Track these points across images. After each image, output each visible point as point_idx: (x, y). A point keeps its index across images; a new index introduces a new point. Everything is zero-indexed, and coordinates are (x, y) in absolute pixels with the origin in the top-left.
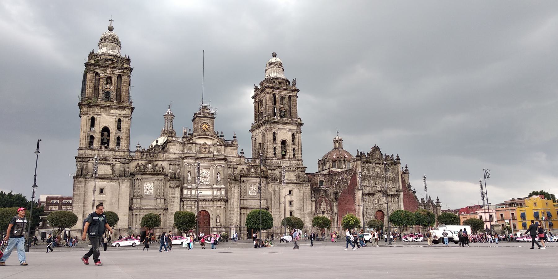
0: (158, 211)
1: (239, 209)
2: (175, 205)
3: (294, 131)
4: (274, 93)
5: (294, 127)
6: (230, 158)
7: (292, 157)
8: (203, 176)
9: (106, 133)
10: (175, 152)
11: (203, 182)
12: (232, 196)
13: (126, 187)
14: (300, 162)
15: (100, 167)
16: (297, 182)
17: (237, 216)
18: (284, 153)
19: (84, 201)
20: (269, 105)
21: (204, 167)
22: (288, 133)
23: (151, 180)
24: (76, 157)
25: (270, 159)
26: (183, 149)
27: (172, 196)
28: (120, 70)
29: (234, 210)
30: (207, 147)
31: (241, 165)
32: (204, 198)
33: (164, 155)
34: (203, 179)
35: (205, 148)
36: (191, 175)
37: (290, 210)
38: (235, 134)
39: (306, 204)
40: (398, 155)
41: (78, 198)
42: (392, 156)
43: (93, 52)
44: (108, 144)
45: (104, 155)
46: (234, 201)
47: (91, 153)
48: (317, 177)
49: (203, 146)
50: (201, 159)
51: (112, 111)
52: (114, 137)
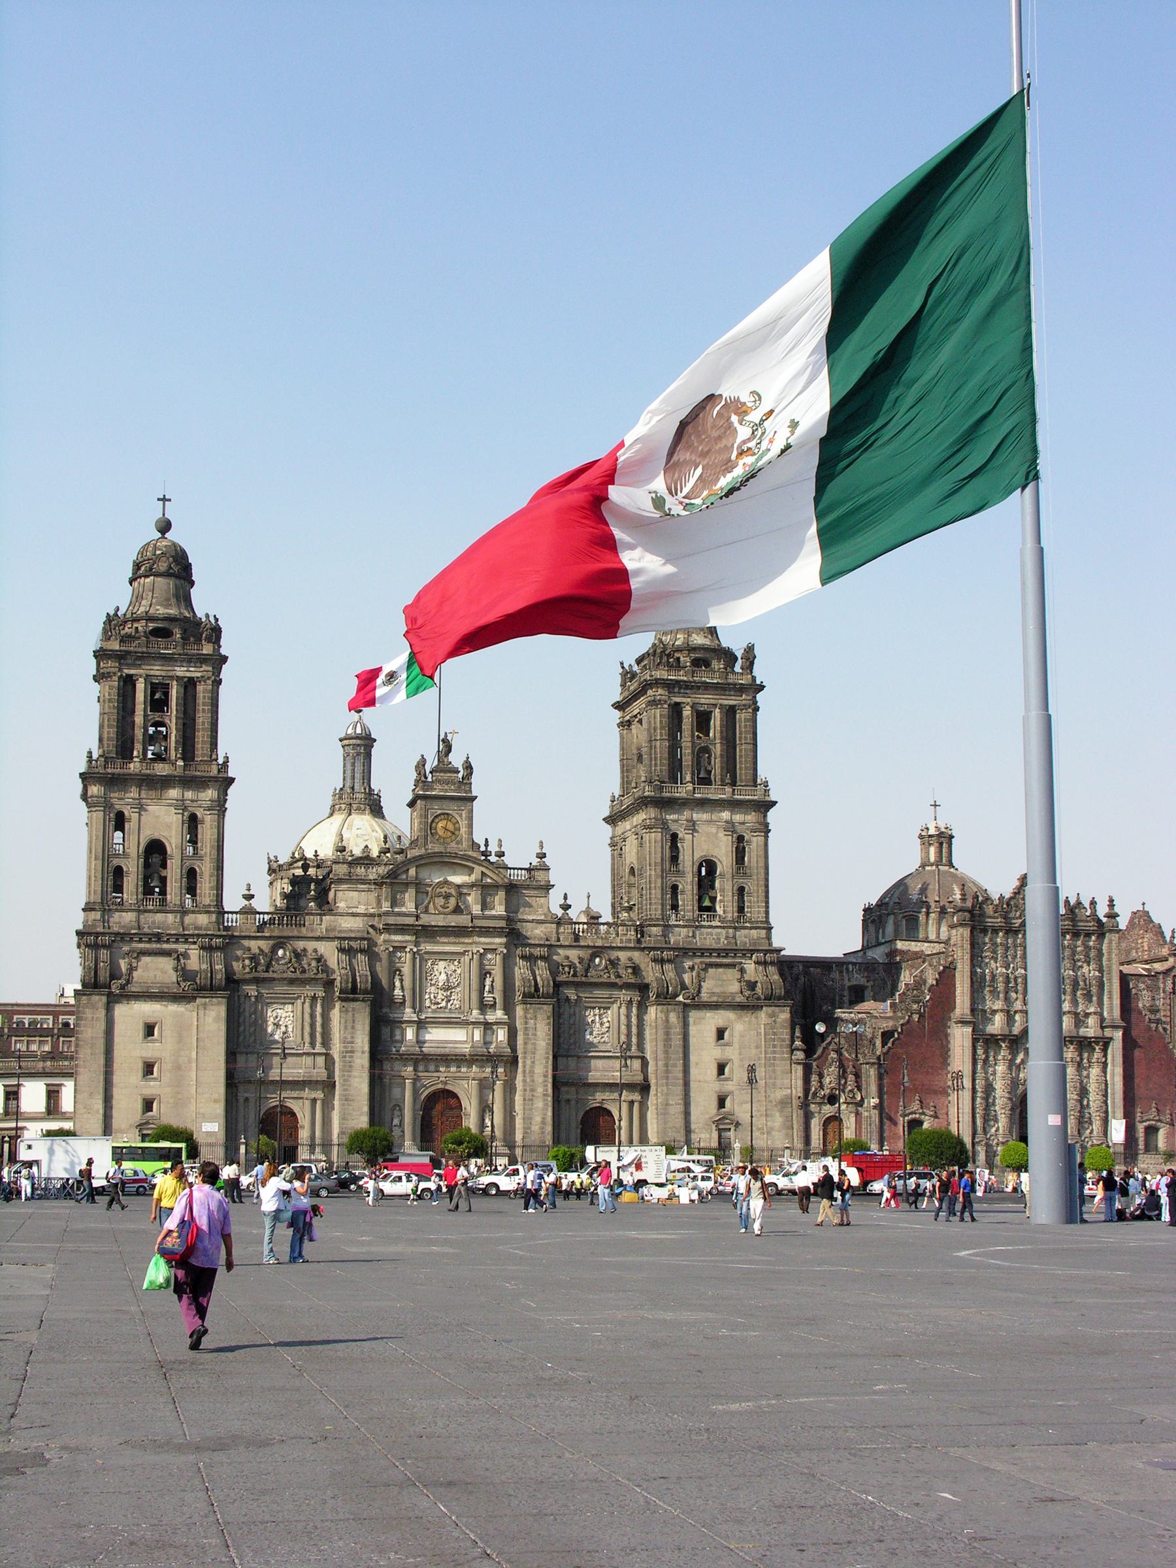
1: (550, 1086)
2: (355, 1073)
9: (156, 859)
10: (354, 910)
11: (439, 1001)
12: (530, 1046)
13: (217, 1019)
15: (146, 960)
18: (707, 903)
20: (658, 743)
22: (721, 834)
27: (345, 1047)
29: (532, 1090)
30: (453, 891)
32: (442, 1051)
33: (321, 920)
35: (447, 896)
36: (401, 981)
37: (717, 1089)
38: (541, 845)
39: (774, 1071)
40: (1111, 901)
41: (89, 1051)
42: (1093, 903)
43: (116, 615)
44: (163, 892)
45: (153, 923)
48: (841, 972)
49: (438, 890)
51: (174, 793)
52: (179, 871)
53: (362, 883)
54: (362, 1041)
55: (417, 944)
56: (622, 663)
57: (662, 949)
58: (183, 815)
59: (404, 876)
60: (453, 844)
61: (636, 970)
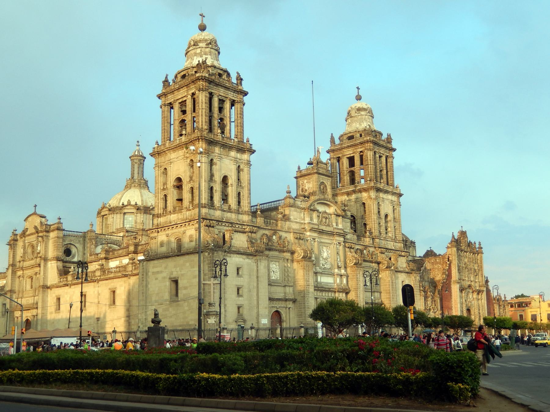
0: (288, 302)
3: (394, 203)
4: (376, 150)
5: (394, 198)
7: (394, 237)
8: (325, 257)
22: (389, 205)
26: (304, 217)
27: (306, 283)
28: (235, 94)
30: (327, 216)
40: (480, 243)
42: (475, 243)
45: (227, 217)
46: (360, 293)
47: (213, 214)
49: (324, 215)
50: (321, 232)
51: (233, 153)
56: (332, 134)
58: (236, 165)
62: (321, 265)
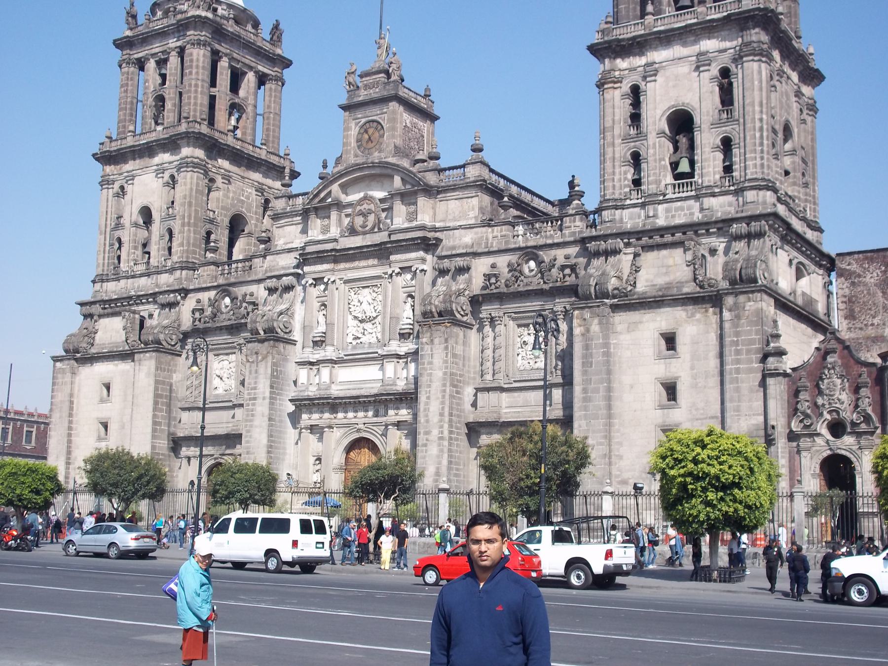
2: (256, 422)
6: (451, 232)
8: (360, 315)
11: (360, 335)
14: (750, 195)
15: (104, 322)
16: (698, 289)
17: (438, 456)
19: (70, 422)
21: (365, 284)
23: (229, 349)
24: (82, 304)
25: (607, 208)
27: (249, 394)
29: (427, 433)
30: (372, 207)
31: (489, 253)
34: (362, 325)
35: (364, 215)
37: (660, 421)
39: (738, 390)
46: (428, 398)
47: (114, 289)
49: (359, 208)
51: (157, 160)
52: (158, 233)
53: (296, 215)
54: (263, 387)
55: (333, 270)
57: (605, 237)
59: (330, 200)
60: (376, 154)
61: (573, 268)
62: (350, 339)
